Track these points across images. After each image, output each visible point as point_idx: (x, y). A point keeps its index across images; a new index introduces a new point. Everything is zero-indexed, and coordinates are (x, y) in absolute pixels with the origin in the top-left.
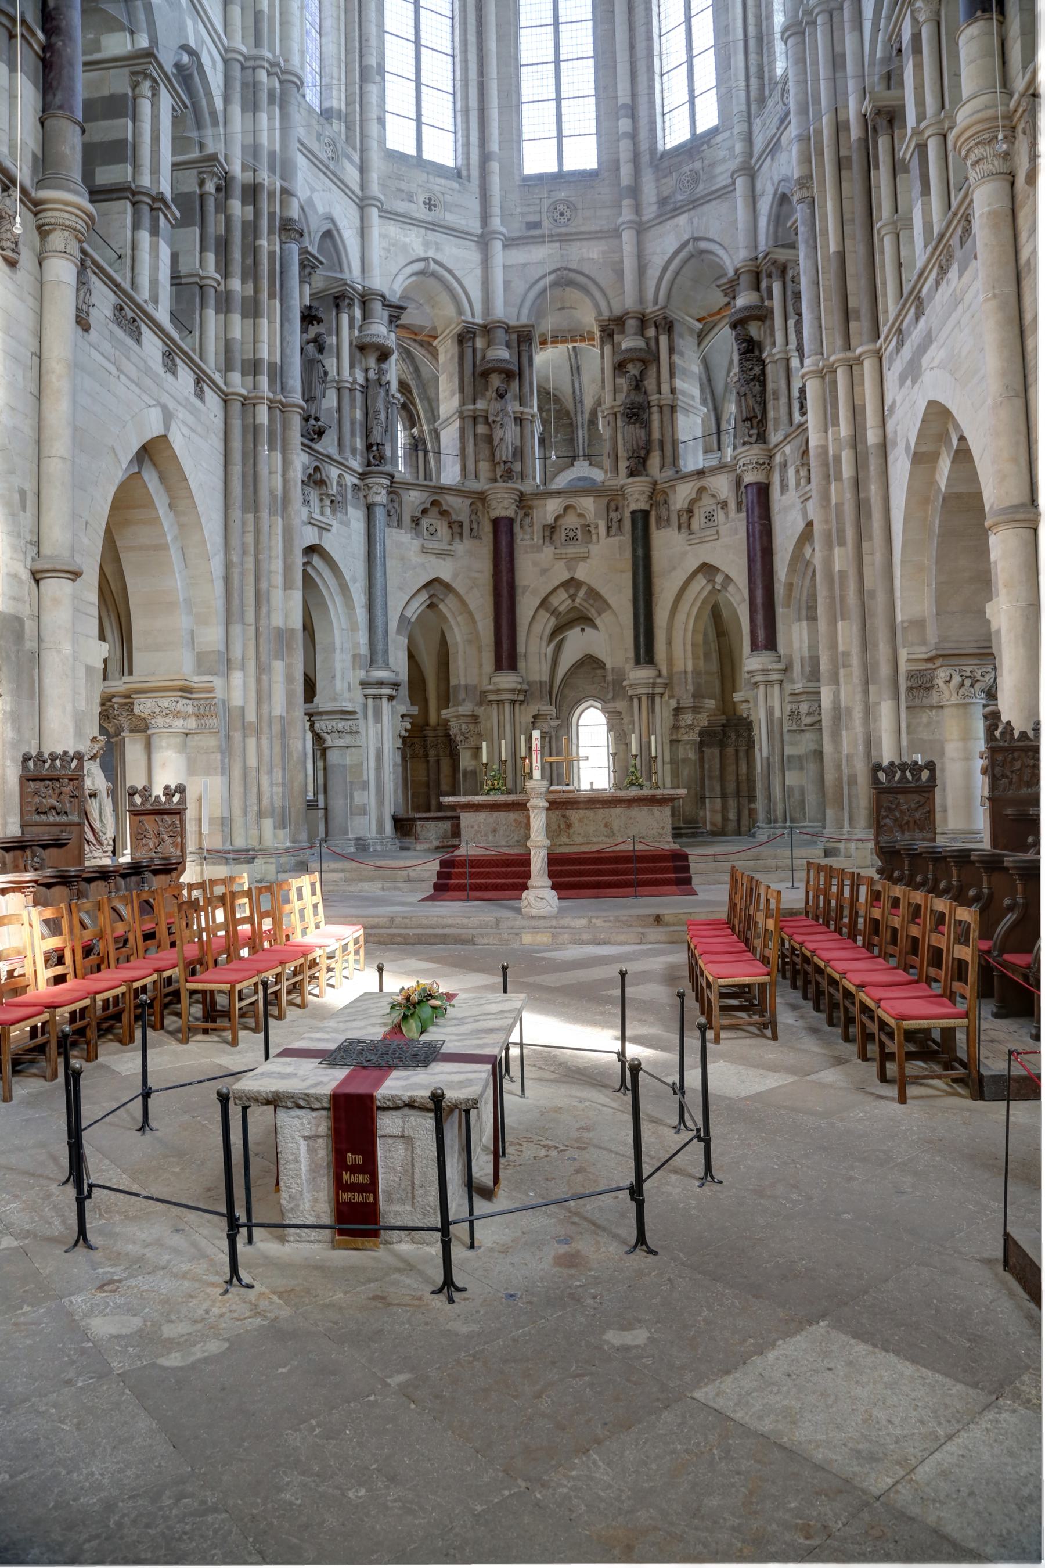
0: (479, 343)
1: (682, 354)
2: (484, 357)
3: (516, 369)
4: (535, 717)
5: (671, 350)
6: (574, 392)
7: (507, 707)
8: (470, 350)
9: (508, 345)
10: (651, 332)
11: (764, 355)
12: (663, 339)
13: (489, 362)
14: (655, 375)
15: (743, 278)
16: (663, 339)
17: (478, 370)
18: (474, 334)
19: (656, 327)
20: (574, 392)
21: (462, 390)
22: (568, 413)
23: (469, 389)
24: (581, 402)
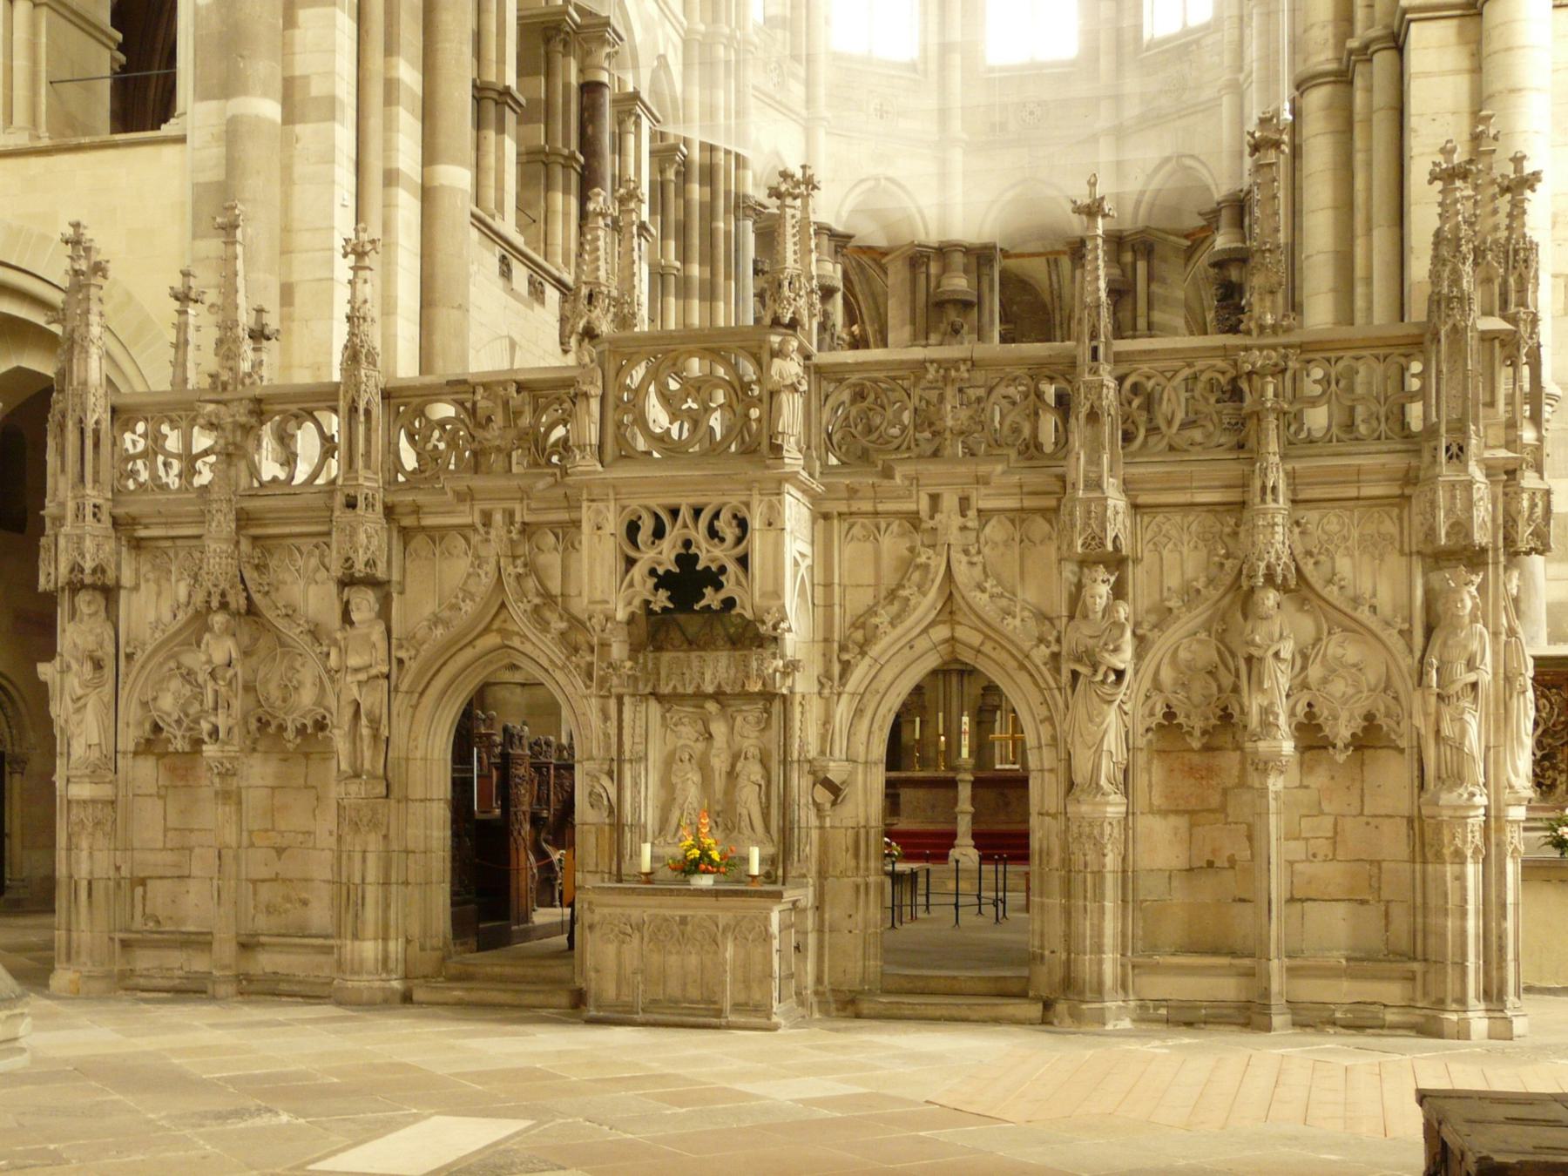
0: (934, 268)
1: (1163, 281)
2: (938, 286)
3: (975, 300)
4: (984, 689)
5: (1150, 278)
6: (1051, 285)
7: (954, 679)
8: (923, 277)
9: (966, 271)
10: (1128, 257)
11: (1243, 302)
12: (1141, 266)
13: (943, 293)
14: (1130, 307)
15: (1224, 212)
16: (1141, 266)
17: (932, 300)
18: (928, 258)
19: (1134, 251)
20: (1051, 285)
21: (913, 322)
22: (1044, 306)
23: (921, 321)
24: (1060, 297)
